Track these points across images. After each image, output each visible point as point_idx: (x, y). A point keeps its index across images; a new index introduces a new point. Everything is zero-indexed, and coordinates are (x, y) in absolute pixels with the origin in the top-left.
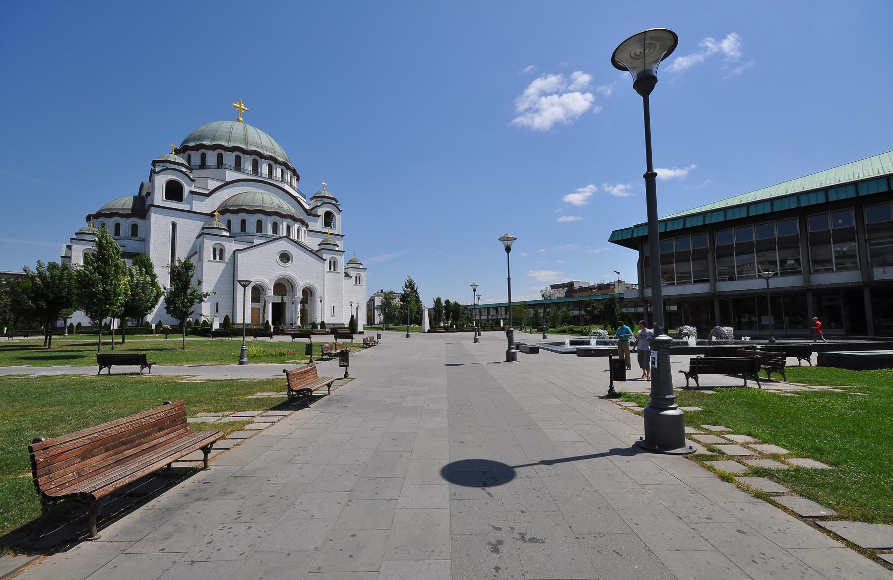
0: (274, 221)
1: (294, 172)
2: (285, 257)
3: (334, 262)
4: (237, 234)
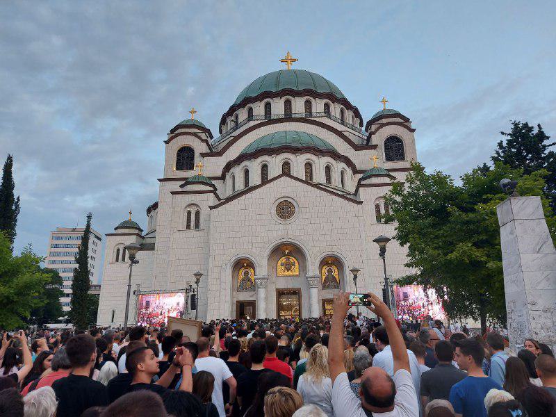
2: (285, 209)
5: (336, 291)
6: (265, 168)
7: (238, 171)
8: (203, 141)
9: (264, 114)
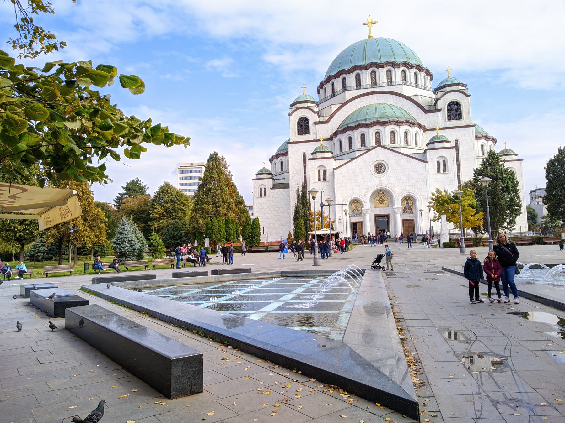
0: (377, 131)
1: (420, 68)
2: (380, 168)
5: (411, 215)
7: (344, 138)
8: (315, 112)
9: (355, 85)
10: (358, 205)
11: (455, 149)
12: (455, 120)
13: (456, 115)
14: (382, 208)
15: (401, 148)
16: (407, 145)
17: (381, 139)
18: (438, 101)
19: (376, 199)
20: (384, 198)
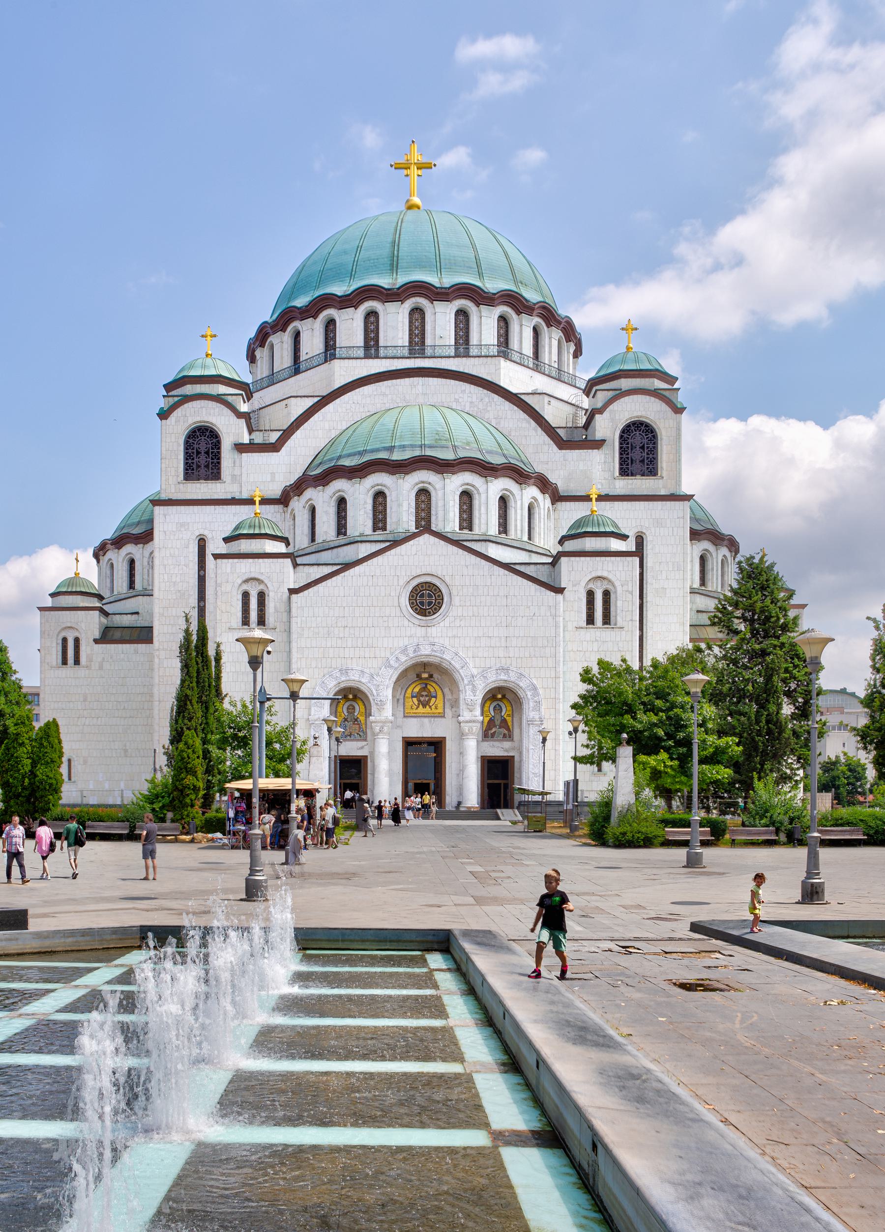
0: (421, 485)
1: (549, 315)
3: (606, 594)
4: (326, 546)
6: (380, 497)
8: (239, 415)
10: (359, 708)
11: (637, 560)
12: (638, 477)
13: (642, 461)
14: (426, 720)
15: (491, 544)
16: (503, 536)
17: (433, 512)
18: (597, 416)
19: (409, 691)
20: (432, 690)
